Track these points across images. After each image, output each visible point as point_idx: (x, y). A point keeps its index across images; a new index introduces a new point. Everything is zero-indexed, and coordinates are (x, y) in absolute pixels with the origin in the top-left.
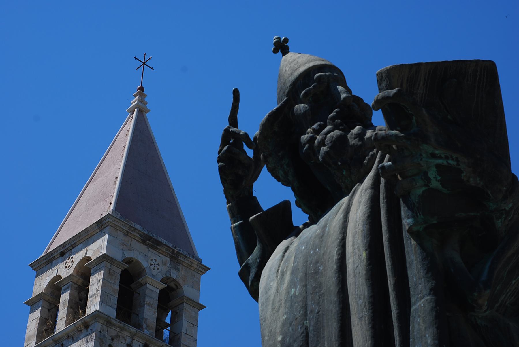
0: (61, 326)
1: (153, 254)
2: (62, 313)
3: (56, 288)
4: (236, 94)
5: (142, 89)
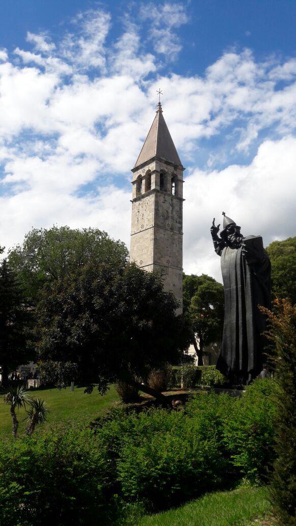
0: (143, 192)
1: (169, 167)
2: (143, 187)
3: (140, 179)
4: (214, 219)
5: (160, 103)
